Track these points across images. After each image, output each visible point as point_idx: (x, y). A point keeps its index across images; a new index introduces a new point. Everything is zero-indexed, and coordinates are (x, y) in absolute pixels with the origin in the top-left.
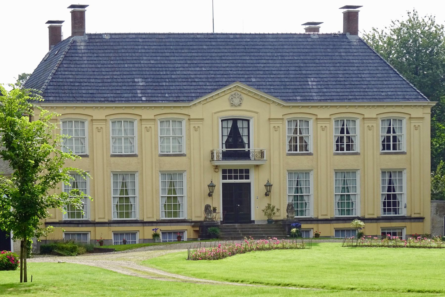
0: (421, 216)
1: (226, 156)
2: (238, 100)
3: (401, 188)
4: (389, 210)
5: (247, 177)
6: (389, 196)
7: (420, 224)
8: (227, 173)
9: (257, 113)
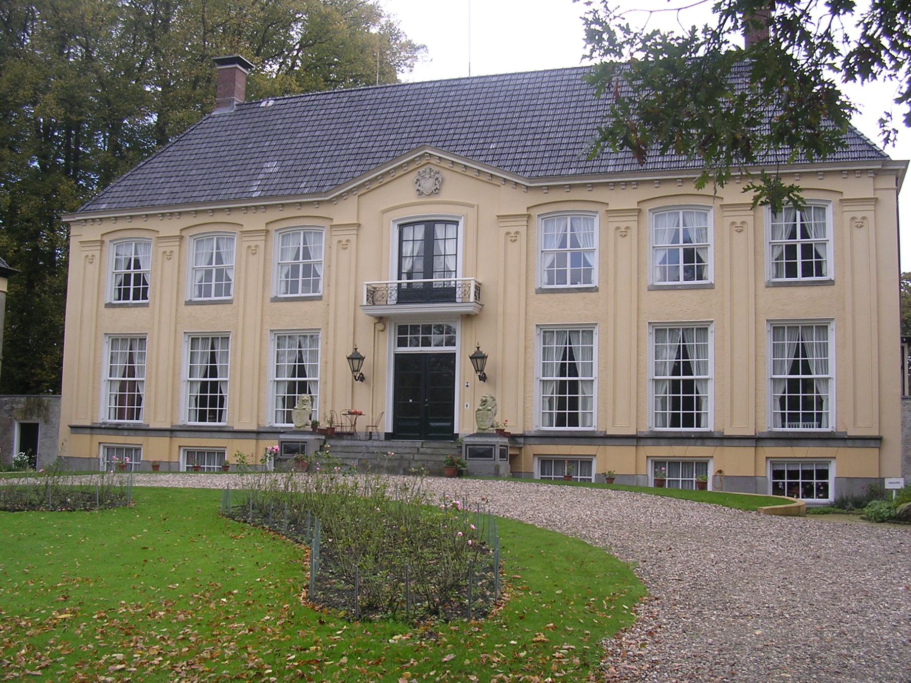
0: (875, 433)
1: (406, 295)
2: (432, 181)
3: (824, 366)
4: (794, 418)
5: (451, 342)
6: (793, 385)
7: (871, 454)
8: (405, 333)
9: (472, 206)
